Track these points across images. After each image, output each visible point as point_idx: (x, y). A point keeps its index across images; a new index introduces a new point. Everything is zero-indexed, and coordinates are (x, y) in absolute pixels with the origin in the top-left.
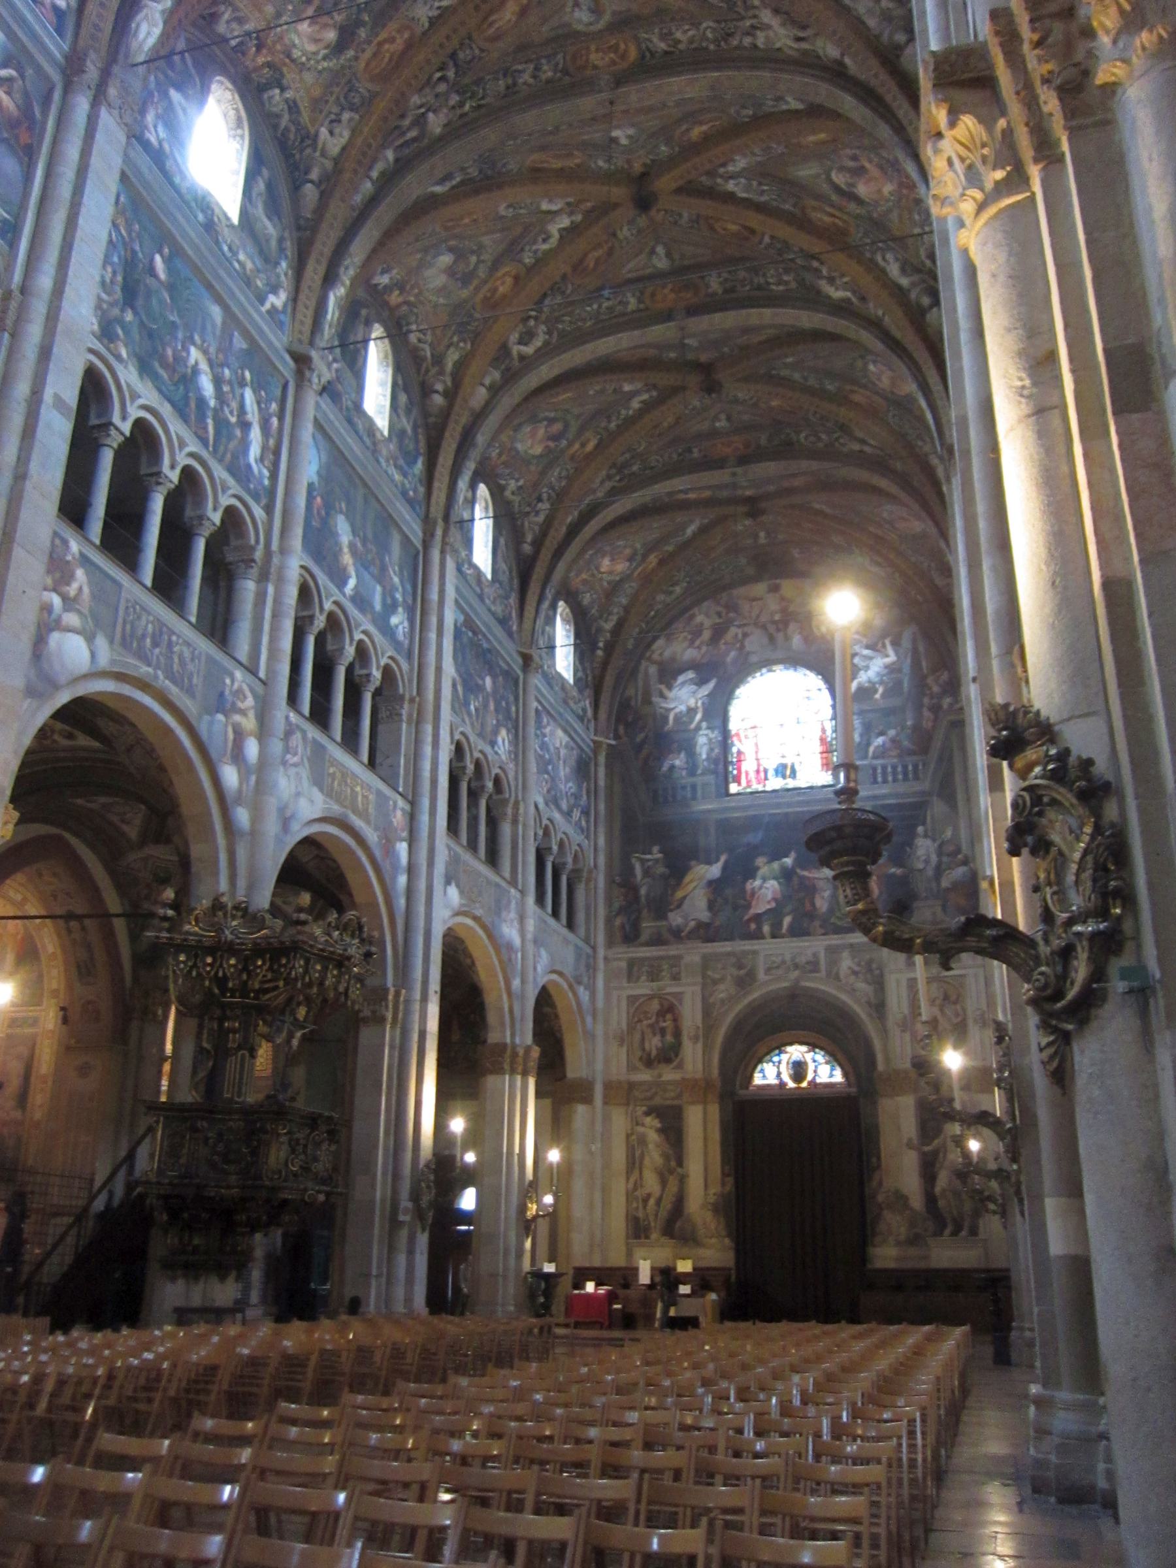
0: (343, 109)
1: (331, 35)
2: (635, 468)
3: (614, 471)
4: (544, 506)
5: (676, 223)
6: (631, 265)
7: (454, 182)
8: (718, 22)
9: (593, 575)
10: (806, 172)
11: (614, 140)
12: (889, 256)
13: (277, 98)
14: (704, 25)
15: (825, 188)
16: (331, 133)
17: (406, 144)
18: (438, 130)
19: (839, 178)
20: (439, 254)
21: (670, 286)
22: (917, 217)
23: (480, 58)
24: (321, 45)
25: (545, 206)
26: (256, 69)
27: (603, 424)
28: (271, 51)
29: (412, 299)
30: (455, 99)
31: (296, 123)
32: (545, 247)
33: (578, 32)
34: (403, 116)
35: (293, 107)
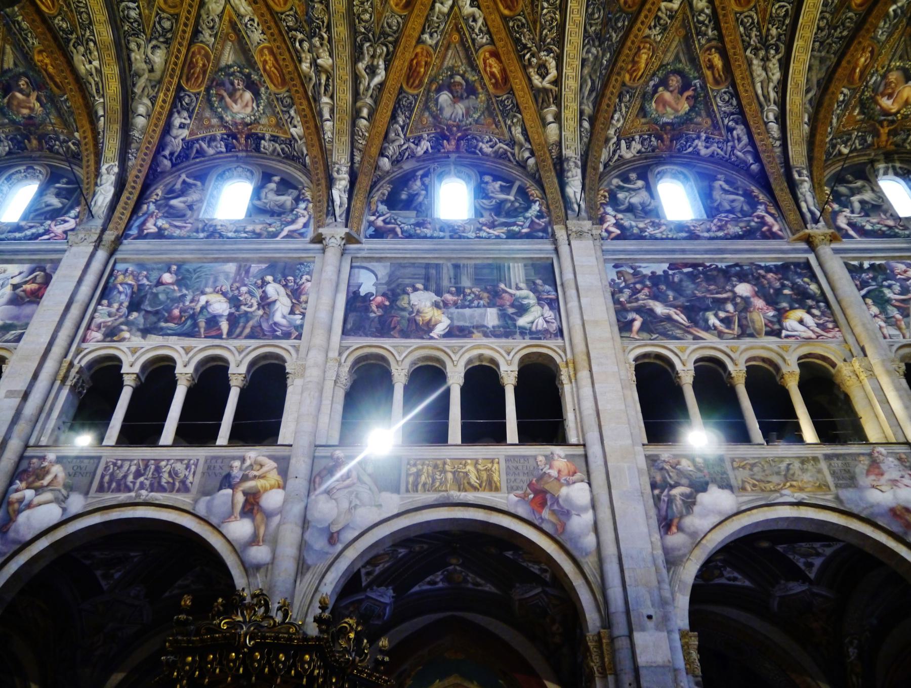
1: (248, 95)
2: (774, 31)
3: (762, 53)
4: (740, 130)
9: (893, 122)
13: (266, 144)
16: (295, 127)
17: (327, 85)
18: (331, 61)
20: (437, 100)
23: (296, 12)
24: (250, 104)
25: (445, 9)
26: (246, 146)
27: (703, 41)
28: (241, 133)
29: (459, 134)
30: (316, 41)
31: (283, 142)
32: (480, 22)
34: (310, 79)
35: (274, 139)
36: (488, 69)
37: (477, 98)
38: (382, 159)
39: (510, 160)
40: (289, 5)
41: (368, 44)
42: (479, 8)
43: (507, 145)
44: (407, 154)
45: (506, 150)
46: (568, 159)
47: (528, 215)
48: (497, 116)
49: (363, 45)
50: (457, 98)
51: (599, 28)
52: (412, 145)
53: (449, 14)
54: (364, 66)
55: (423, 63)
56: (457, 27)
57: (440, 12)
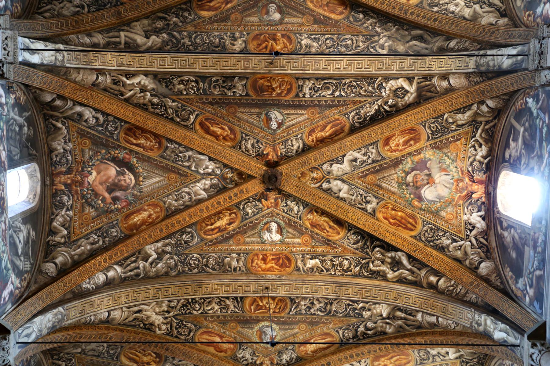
0: (433, 356)
5: (258, 142)
6: (301, 119)
7: (393, 254)
8: (190, 313)
10: (153, 181)
11: (280, 230)
12: (93, 121)
14: (199, 312)
15: (140, 168)
19: (129, 178)
20: (428, 201)
21: (274, 94)
22: (70, 158)
23: (341, 328)
25: (345, 187)
29: (467, 180)
30: (366, 314)
32: (357, 155)
33: (277, 324)
34: (401, 327)
36: (400, 148)
37: (430, 160)
38: (480, 270)
39: (494, 126)
40: (334, 333)
41: (371, 265)
42: (344, 156)
43: (477, 129)
44: (482, 240)
45: (483, 130)
46: (478, 66)
47: (535, 112)
48: (447, 139)
49: (371, 270)
50: (430, 180)
51: (361, 38)
52: (474, 232)
53: (349, 184)
54: (391, 272)
55: (393, 212)
56: (361, 177)
57: (348, 193)
